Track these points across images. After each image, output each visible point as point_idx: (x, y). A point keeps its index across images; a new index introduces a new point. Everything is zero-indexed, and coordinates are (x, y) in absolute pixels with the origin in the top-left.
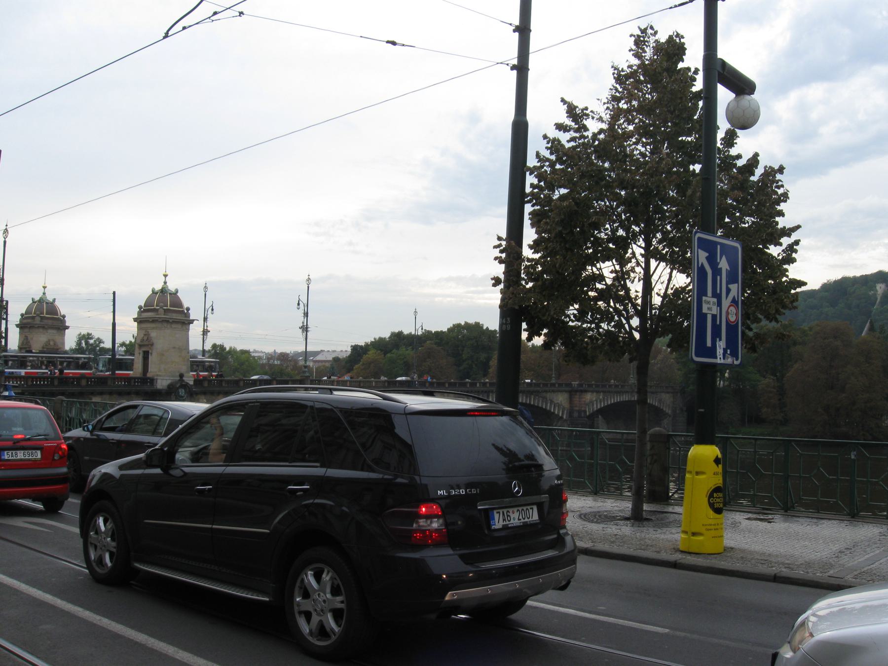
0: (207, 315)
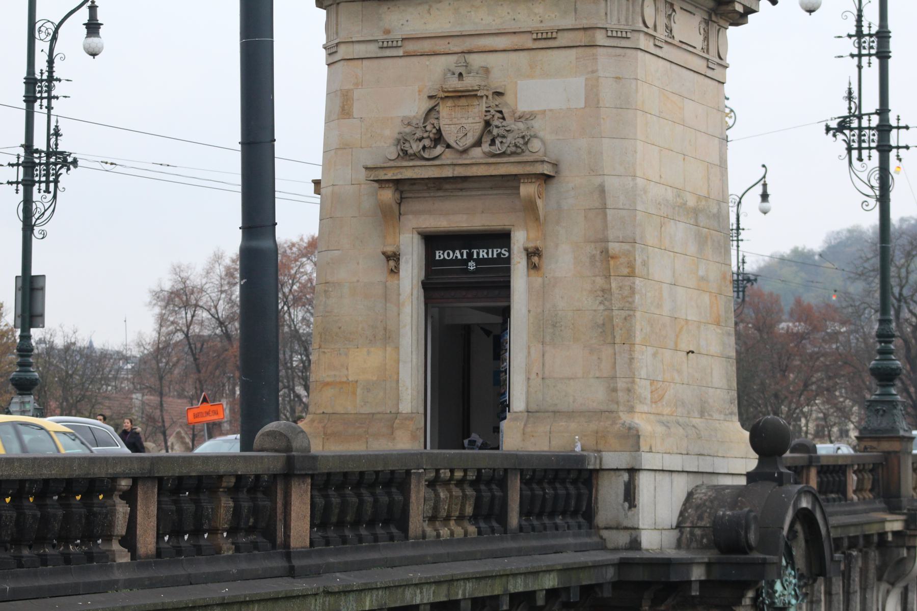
0: (51, 62)
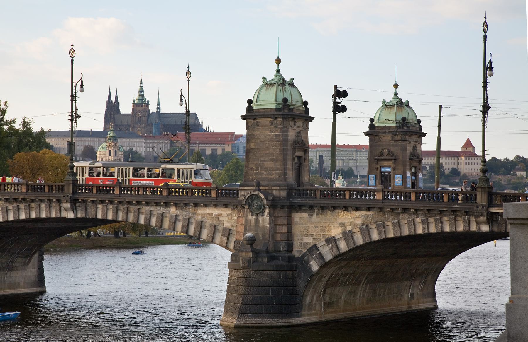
0: (75, 92)
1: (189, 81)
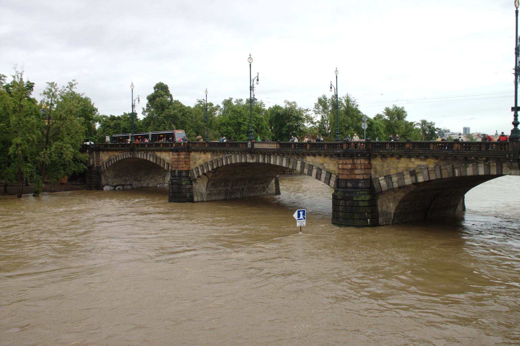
0: (253, 85)
1: (337, 77)
